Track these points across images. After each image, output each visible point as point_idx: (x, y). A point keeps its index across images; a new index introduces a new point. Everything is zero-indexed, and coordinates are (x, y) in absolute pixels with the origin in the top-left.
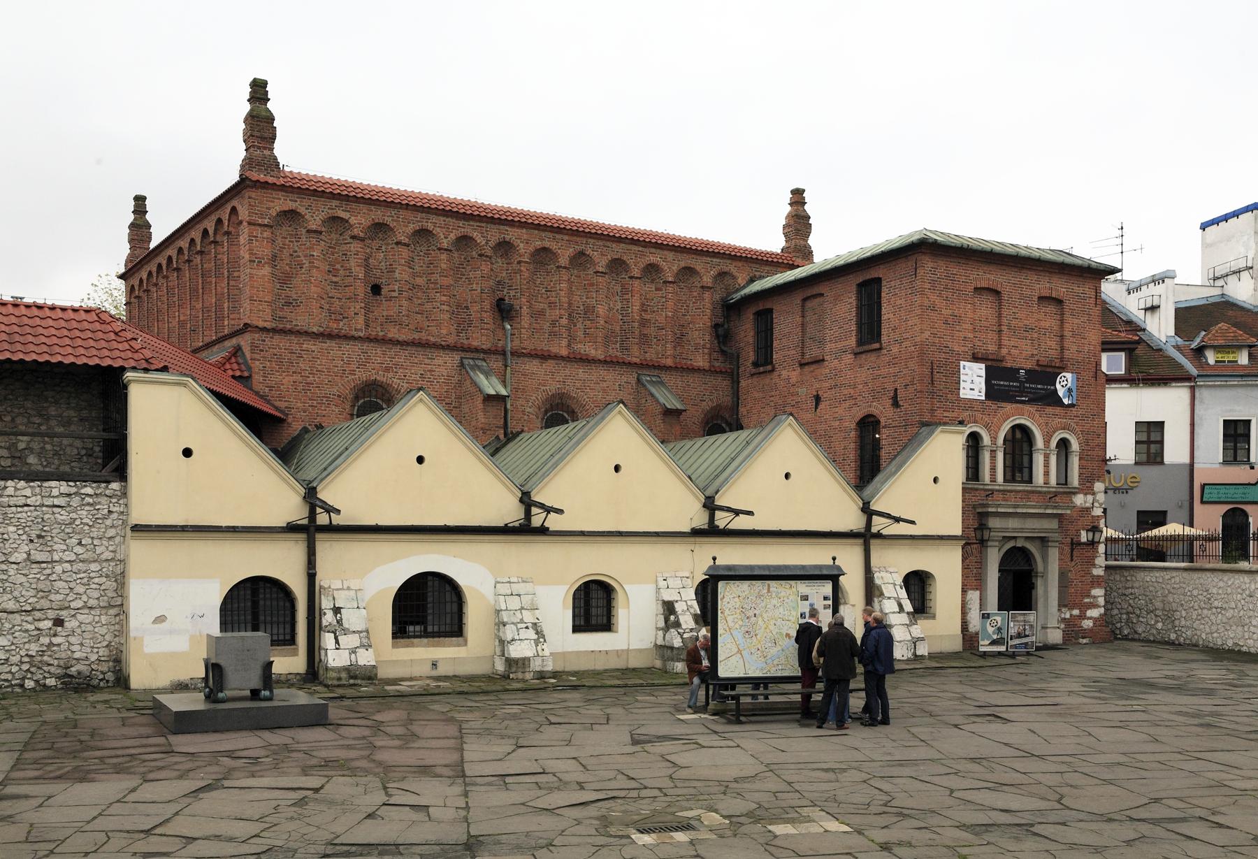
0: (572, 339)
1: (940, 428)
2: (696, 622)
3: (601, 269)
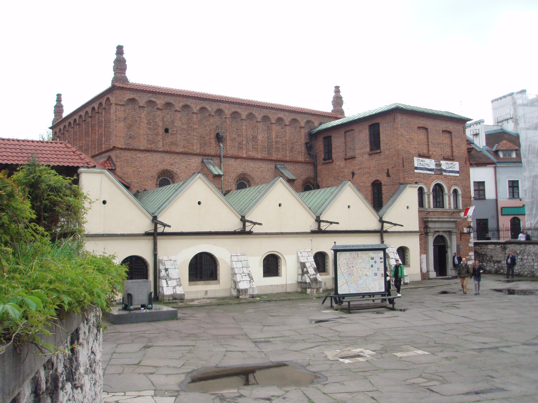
0: (248, 150)
1: (408, 185)
2: (315, 271)
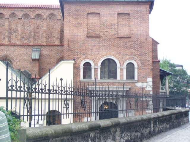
3: (20, 18)
